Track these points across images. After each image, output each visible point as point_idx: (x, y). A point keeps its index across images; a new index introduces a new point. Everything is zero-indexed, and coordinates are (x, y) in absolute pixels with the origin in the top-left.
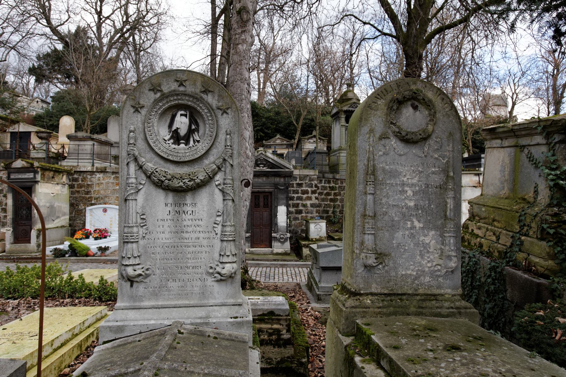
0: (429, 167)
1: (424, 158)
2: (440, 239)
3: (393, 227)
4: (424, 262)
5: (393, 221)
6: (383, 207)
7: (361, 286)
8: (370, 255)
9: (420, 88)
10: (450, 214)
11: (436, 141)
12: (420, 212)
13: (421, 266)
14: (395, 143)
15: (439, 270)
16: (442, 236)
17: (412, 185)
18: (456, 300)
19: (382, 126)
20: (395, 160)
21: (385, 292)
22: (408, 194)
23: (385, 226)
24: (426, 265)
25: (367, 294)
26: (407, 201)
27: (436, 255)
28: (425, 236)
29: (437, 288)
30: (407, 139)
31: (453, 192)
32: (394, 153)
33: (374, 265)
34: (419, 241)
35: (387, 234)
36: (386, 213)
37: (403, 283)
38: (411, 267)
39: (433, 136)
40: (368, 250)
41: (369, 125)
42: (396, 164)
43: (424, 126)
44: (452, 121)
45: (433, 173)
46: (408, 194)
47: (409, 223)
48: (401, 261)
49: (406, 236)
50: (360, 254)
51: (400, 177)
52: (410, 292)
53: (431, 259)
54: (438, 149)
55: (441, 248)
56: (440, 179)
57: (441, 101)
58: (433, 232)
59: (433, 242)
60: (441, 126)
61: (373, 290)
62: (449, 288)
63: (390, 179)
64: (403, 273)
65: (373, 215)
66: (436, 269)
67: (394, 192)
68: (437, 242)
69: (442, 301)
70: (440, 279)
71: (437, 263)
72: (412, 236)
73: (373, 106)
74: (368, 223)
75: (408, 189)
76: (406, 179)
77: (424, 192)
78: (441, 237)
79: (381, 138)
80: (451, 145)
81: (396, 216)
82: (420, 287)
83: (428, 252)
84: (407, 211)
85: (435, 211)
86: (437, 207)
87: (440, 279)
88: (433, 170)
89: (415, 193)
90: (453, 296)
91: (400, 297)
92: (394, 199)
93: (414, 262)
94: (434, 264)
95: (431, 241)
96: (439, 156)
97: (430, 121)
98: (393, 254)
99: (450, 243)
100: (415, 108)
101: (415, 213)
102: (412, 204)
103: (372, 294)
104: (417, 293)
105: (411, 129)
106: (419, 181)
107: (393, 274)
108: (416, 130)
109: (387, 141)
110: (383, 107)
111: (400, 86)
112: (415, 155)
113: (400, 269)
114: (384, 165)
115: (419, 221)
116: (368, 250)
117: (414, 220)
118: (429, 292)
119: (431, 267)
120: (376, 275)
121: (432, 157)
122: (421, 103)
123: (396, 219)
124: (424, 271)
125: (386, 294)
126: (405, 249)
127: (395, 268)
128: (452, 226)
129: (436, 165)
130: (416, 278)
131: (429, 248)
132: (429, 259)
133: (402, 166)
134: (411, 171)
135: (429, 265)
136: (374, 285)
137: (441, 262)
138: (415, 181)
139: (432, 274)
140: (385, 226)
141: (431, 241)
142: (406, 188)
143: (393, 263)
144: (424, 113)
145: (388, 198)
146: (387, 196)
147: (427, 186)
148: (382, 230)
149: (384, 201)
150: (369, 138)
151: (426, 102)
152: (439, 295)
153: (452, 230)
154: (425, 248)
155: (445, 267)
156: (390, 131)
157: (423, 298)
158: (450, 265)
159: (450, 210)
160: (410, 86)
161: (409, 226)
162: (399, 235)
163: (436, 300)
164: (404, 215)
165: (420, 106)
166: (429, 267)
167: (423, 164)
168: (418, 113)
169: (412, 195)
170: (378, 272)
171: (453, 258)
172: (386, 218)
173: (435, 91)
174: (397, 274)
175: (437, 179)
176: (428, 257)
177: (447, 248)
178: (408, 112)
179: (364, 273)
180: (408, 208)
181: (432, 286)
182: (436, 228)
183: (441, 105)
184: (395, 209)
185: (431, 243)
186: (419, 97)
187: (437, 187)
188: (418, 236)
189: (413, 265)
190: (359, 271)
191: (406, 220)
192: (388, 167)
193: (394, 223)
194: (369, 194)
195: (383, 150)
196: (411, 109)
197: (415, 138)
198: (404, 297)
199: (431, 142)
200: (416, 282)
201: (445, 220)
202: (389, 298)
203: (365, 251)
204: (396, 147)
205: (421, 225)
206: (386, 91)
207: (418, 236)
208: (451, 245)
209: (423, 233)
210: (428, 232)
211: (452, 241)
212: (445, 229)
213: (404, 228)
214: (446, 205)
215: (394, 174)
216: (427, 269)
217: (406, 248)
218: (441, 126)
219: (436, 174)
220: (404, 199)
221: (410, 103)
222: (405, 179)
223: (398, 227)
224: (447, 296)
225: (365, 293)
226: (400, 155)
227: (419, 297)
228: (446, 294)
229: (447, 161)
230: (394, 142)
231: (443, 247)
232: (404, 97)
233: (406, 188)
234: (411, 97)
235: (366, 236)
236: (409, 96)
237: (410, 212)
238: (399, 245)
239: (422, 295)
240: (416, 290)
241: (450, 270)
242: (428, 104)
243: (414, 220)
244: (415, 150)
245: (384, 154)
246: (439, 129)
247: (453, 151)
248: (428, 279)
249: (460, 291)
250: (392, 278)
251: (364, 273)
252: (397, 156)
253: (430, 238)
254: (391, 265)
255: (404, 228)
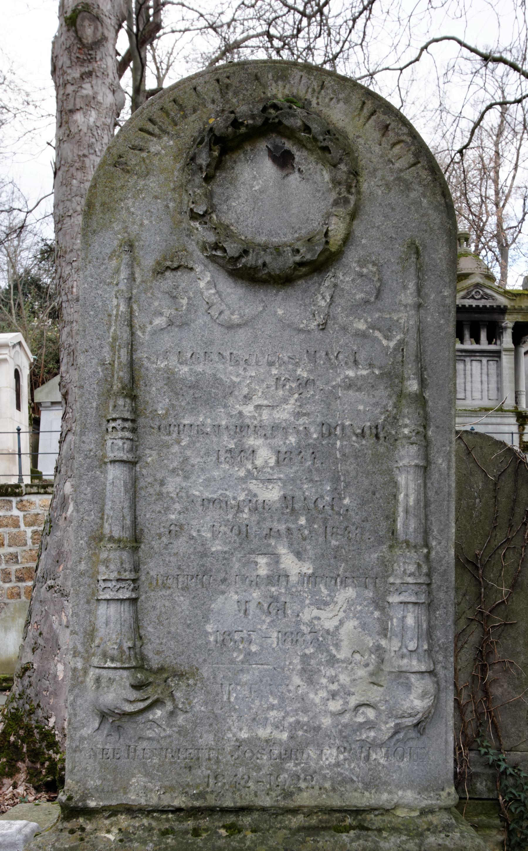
0: (334, 367)
1: (318, 335)
2: (377, 614)
3: (206, 576)
4: (317, 697)
5: (204, 555)
6: (167, 509)
7: (91, 783)
8: (111, 674)
9: (302, 93)
10: (406, 525)
11: (361, 275)
12: (302, 521)
13: (305, 711)
14: (213, 284)
15: (370, 725)
16: (380, 603)
17: (275, 427)
18: (432, 829)
19: (166, 229)
20: (212, 342)
21: (176, 803)
22: (259, 462)
23: (176, 572)
24: (325, 706)
25: (113, 811)
26: (253, 486)
27: (361, 672)
28: (322, 604)
29: (367, 786)
30: (254, 271)
31: (413, 449)
32: (207, 319)
33: (129, 708)
34: (298, 623)
35: (183, 602)
36: (176, 530)
37: (241, 770)
38: (273, 714)
39: (352, 257)
40: (105, 655)
41: (117, 227)
42: (215, 357)
43: (316, 224)
44: (417, 203)
45: (350, 385)
46: (259, 462)
47: (262, 561)
48: (234, 695)
49: (252, 606)
50: (85, 672)
51: (231, 401)
52: (266, 802)
53: (342, 686)
54: (367, 302)
55: (378, 648)
56: (376, 404)
57: (377, 135)
58: (350, 592)
59: (351, 624)
60: (378, 220)
61: (134, 798)
62: (411, 786)
63: (193, 411)
64: (244, 735)
65: (127, 535)
66: (360, 719)
67: (207, 454)
68: (364, 626)
69: (380, 830)
70: (378, 756)
71: (363, 699)
72: (275, 607)
73: (133, 159)
74: (106, 562)
75: (260, 442)
76: (251, 408)
77: (315, 451)
78: (378, 607)
79: (160, 271)
80: (412, 286)
81: (214, 537)
82: (303, 785)
83: (332, 661)
84: (255, 518)
85: (356, 519)
86: (363, 503)
87: (378, 756)
88: (351, 373)
89: (283, 458)
90: (424, 812)
91: (231, 819)
92: (208, 481)
93: (282, 699)
94: (353, 701)
95: (341, 623)
96: (374, 328)
97: (336, 203)
98: (205, 671)
99: (403, 628)
100: (283, 160)
101: (282, 527)
102: (272, 494)
103: (130, 810)
104: (291, 804)
105: (270, 234)
106: (298, 415)
107: (207, 739)
108: (288, 238)
109: (182, 279)
110: (168, 161)
111: (227, 86)
112: (285, 325)
113: (232, 720)
114: (173, 360)
115: (299, 555)
116: (105, 655)
117: (282, 550)
118: (336, 802)
119: (342, 713)
120: (145, 744)
121: (344, 329)
122: (302, 145)
123: (217, 547)
124: (317, 729)
125: (179, 810)
126: (249, 654)
127: (215, 720)
128: (412, 568)
129: (362, 357)
130: (290, 753)
131: (337, 646)
132: (334, 687)
133: (237, 363)
134: (271, 382)
135: (335, 706)
136: (138, 780)
137: (375, 694)
138: (284, 414)
139: (347, 737)
140: (176, 572)
141: (341, 623)
142: (252, 441)
143: (206, 703)
144: (318, 177)
145: (186, 478)
146: (185, 470)
147: (329, 431)
148: (165, 586)
149: (172, 485)
150: (117, 271)
151: (315, 139)
152: (372, 810)
153: (410, 580)
154: (320, 647)
155: (391, 714)
156: (193, 247)
157: (314, 821)
158: (406, 705)
159: (407, 511)
160: (265, 86)
161: (263, 571)
162: (227, 602)
163: (362, 828)
164: (244, 534)
165: (299, 155)
166: (334, 714)
167: (312, 356)
168: (295, 177)
169: (272, 462)
170: (150, 734)
171: (413, 678)
172: (181, 545)
173: (356, 99)
174: (219, 739)
175: (362, 407)
176: (333, 680)
177: (395, 645)
178: (255, 175)
179: (100, 738)
180: (260, 508)
181: (346, 781)
182: (360, 577)
183: (377, 149)
184: (213, 515)
185: (343, 631)
186: (289, 122)
187: (363, 434)
188: (297, 607)
189: (279, 708)
190: (86, 732)
191: (252, 552)
192: (185, 369)
193: (208, 561)
194: (113, 462)
195: (167, 312)
196: (268, 167)
197: (276, 265)
198: (246, 820)
199: (345, 276)
200: (290, 765)
201: (391, 547)
202: (190, 824)
203: (95, 661)
204: (215, 299)
205: (308, 568)
206: (181, 108)
207: (297, 607)
208: (409, 634)
209: (313, 594)
210: (332, 592)
211: (410, 621)
212: (391, 580)
213: (244, 579)
214: (395, 496)
215: (208, 393)
216: (326, 722)
217: (254, 648)
218: (378, 220)
219: (359, 390)
220: (244, 480)
221: (263, 145)
222: (248, 410)
223: (222, 575)
224: (401, 813)
225: (104, 809)
226: (231, 327)
227: (301, 817)
228: (396, 806)
229: (402, 342)
230: (206, 282)
231: (383, 643)
232: (236, 124)
233: (252, 441)
234: (259, 121)
235: (102, 610)
236: (253, 117)
237: (267, 525)
238: (226, 640)
239: (310, 812)
240: (288, 795)
241: (409, 721)
242: (330, 146)
243: (282, 550)
244: (282, 307)
245: (171, 323)
246: (373, 232)
247: (419, 306)
248: (331, 755)
249: (449, 795)
250: (204, 754)
251: (100, 738)
252: (218, 332)
253: (339, 613)
254: (199, 707)
255: (244, 579)
